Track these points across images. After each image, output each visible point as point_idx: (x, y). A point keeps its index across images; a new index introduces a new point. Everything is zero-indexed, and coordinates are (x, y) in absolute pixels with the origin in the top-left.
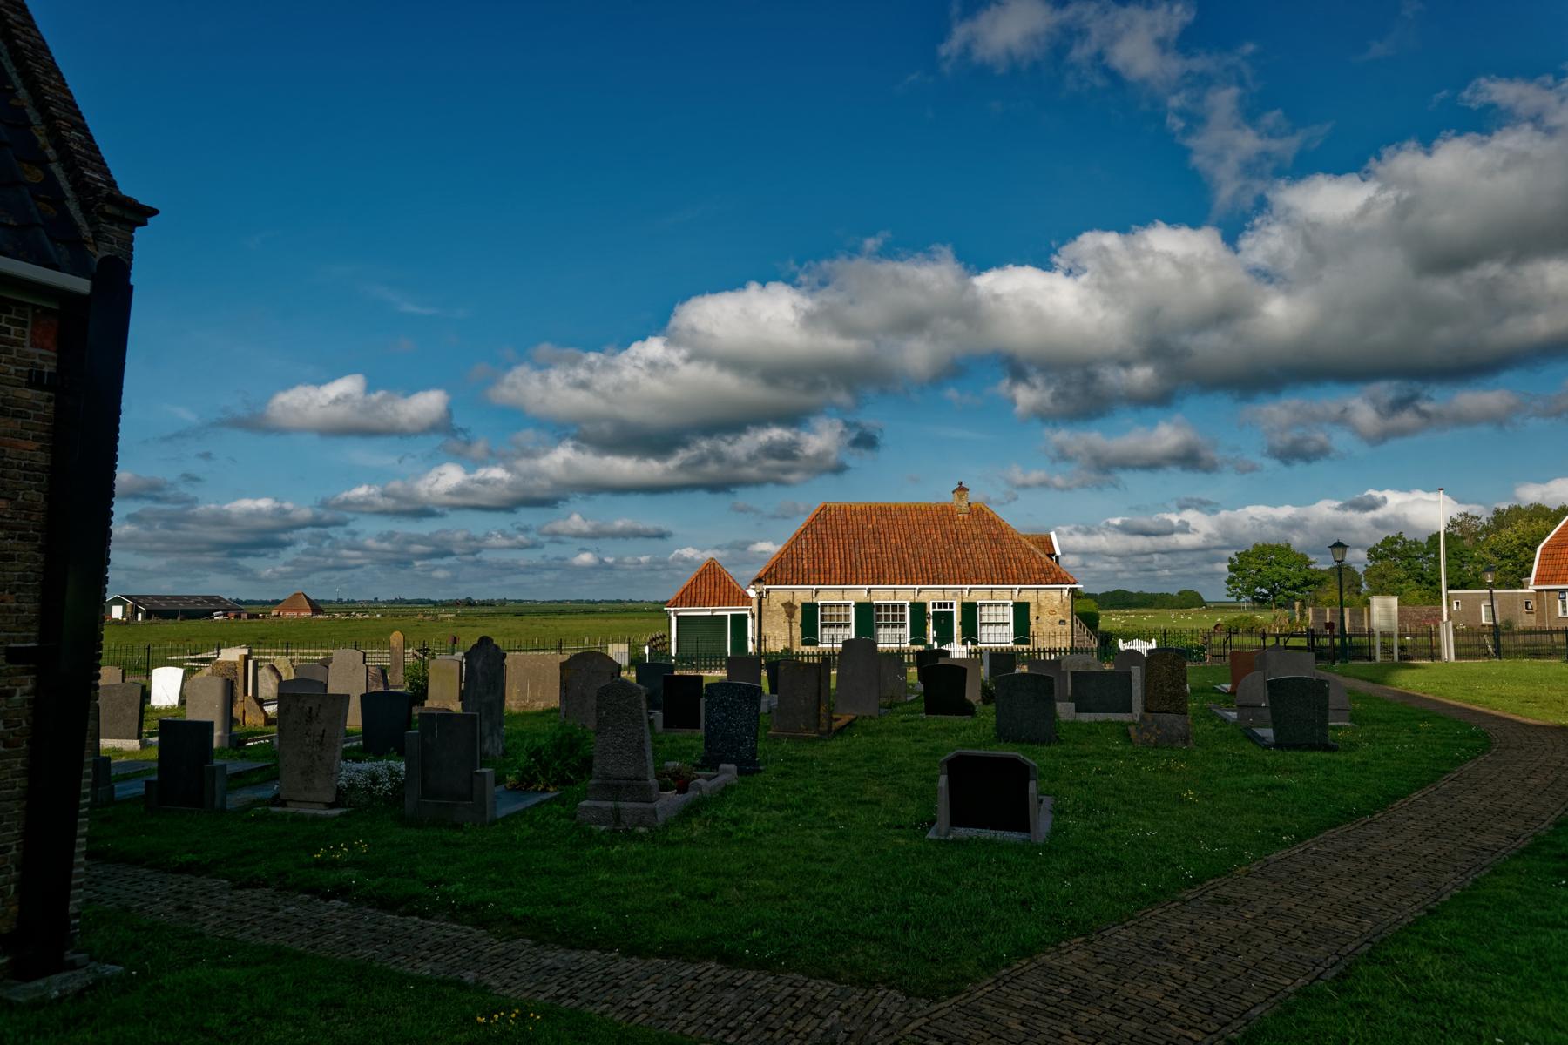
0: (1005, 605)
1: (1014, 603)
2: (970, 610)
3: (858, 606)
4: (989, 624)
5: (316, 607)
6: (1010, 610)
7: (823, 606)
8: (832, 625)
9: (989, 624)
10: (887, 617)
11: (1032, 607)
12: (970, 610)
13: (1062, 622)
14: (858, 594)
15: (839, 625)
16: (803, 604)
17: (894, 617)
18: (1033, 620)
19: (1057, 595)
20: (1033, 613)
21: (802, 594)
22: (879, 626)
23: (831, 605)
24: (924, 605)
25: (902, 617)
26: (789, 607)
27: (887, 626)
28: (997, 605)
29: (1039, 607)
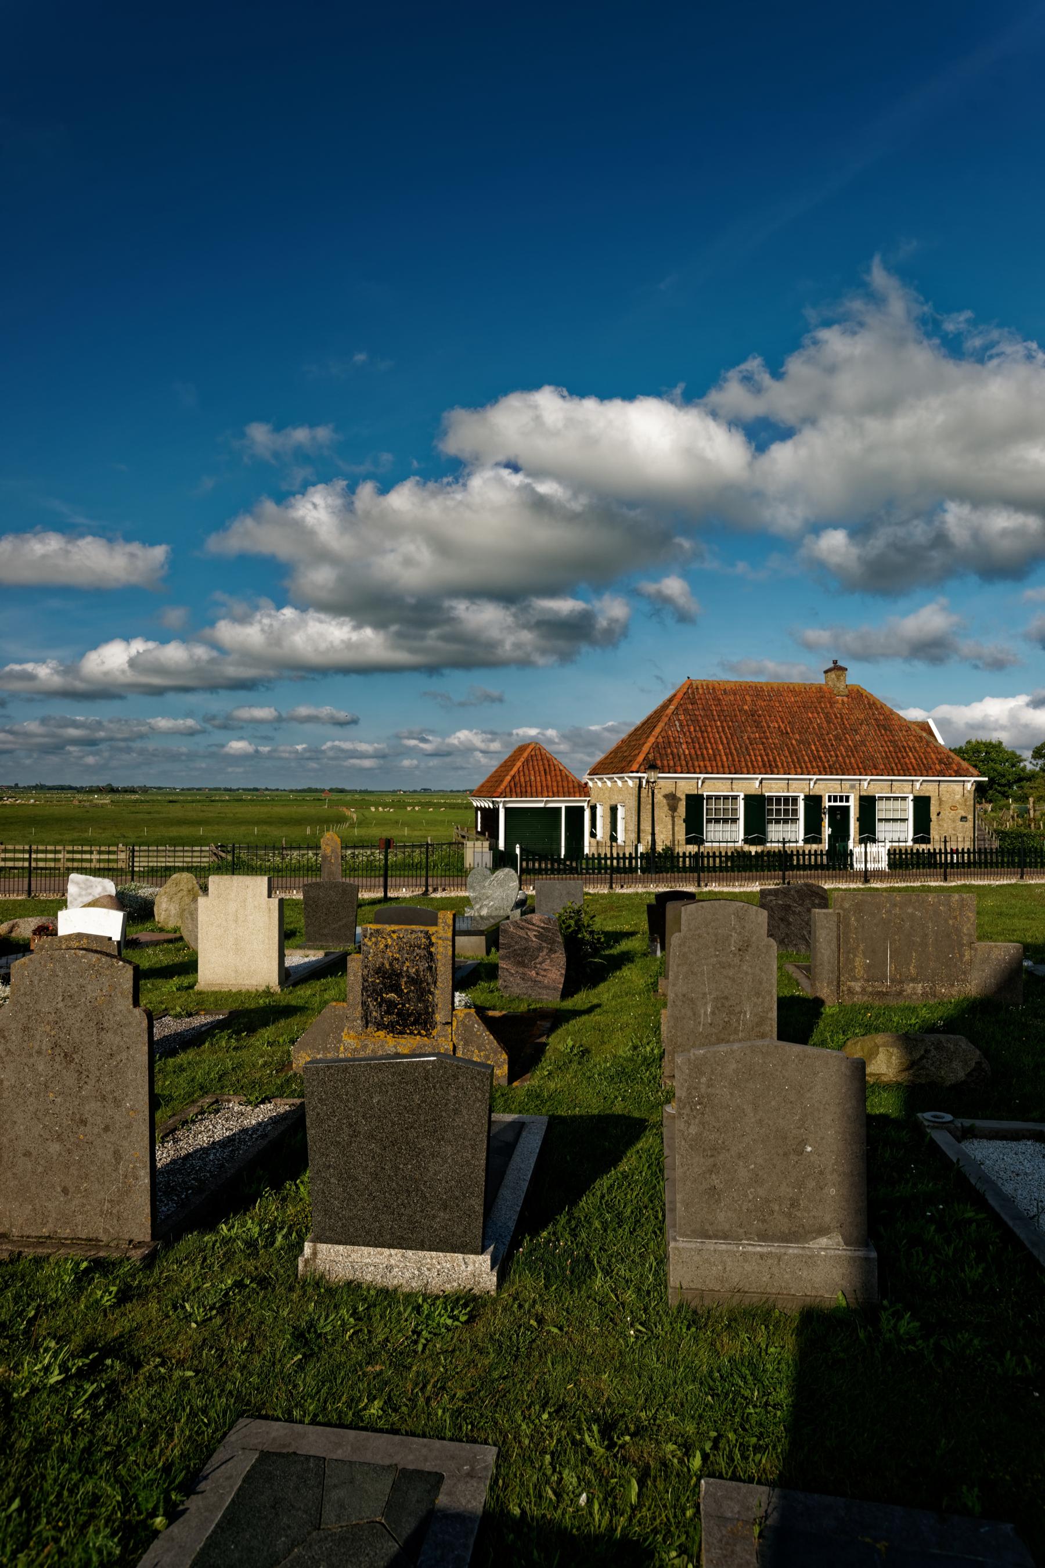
0: (904, 799)
1: (805, 796)
2: (868, 804)
3: (748, 798)
4: (887, 820)
6: (910, 805)
7: (709, 797)
8: (717, 821)
9: (887, 820)
10: (778, 811)
11: (933, 802)
12: (868, 804)
13: (964, 819)
14: (751, 784)
15: (725, 821)
16: (688, 797)
17: (786, 811)
18: (933, 816)
19: (958, 788)
20: (934, 809)
21: (686, 784)
22: (770, 821)
23: (718, 798)
24: (819, 799)
25: (795, 812)
26: (672, 799)
27: (778, 822)
28: (896, 799)
29: (940, 802)
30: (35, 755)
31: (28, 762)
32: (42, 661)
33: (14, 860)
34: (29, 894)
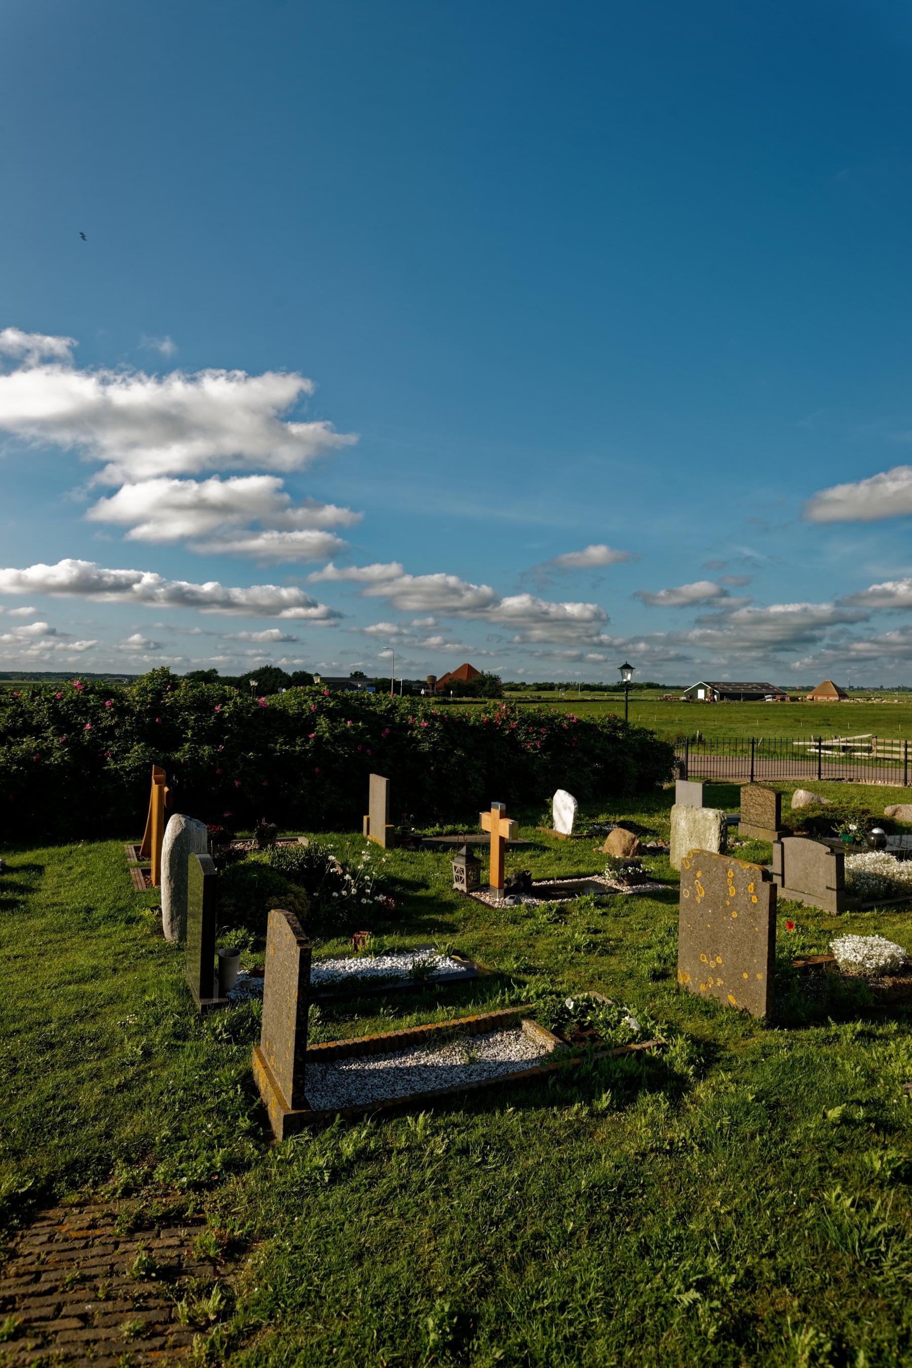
5: (842, 694)
30: (897, 661)
31: (891, 667)
32: (898, 579)
33: (892, 752)
34: (906, 783)
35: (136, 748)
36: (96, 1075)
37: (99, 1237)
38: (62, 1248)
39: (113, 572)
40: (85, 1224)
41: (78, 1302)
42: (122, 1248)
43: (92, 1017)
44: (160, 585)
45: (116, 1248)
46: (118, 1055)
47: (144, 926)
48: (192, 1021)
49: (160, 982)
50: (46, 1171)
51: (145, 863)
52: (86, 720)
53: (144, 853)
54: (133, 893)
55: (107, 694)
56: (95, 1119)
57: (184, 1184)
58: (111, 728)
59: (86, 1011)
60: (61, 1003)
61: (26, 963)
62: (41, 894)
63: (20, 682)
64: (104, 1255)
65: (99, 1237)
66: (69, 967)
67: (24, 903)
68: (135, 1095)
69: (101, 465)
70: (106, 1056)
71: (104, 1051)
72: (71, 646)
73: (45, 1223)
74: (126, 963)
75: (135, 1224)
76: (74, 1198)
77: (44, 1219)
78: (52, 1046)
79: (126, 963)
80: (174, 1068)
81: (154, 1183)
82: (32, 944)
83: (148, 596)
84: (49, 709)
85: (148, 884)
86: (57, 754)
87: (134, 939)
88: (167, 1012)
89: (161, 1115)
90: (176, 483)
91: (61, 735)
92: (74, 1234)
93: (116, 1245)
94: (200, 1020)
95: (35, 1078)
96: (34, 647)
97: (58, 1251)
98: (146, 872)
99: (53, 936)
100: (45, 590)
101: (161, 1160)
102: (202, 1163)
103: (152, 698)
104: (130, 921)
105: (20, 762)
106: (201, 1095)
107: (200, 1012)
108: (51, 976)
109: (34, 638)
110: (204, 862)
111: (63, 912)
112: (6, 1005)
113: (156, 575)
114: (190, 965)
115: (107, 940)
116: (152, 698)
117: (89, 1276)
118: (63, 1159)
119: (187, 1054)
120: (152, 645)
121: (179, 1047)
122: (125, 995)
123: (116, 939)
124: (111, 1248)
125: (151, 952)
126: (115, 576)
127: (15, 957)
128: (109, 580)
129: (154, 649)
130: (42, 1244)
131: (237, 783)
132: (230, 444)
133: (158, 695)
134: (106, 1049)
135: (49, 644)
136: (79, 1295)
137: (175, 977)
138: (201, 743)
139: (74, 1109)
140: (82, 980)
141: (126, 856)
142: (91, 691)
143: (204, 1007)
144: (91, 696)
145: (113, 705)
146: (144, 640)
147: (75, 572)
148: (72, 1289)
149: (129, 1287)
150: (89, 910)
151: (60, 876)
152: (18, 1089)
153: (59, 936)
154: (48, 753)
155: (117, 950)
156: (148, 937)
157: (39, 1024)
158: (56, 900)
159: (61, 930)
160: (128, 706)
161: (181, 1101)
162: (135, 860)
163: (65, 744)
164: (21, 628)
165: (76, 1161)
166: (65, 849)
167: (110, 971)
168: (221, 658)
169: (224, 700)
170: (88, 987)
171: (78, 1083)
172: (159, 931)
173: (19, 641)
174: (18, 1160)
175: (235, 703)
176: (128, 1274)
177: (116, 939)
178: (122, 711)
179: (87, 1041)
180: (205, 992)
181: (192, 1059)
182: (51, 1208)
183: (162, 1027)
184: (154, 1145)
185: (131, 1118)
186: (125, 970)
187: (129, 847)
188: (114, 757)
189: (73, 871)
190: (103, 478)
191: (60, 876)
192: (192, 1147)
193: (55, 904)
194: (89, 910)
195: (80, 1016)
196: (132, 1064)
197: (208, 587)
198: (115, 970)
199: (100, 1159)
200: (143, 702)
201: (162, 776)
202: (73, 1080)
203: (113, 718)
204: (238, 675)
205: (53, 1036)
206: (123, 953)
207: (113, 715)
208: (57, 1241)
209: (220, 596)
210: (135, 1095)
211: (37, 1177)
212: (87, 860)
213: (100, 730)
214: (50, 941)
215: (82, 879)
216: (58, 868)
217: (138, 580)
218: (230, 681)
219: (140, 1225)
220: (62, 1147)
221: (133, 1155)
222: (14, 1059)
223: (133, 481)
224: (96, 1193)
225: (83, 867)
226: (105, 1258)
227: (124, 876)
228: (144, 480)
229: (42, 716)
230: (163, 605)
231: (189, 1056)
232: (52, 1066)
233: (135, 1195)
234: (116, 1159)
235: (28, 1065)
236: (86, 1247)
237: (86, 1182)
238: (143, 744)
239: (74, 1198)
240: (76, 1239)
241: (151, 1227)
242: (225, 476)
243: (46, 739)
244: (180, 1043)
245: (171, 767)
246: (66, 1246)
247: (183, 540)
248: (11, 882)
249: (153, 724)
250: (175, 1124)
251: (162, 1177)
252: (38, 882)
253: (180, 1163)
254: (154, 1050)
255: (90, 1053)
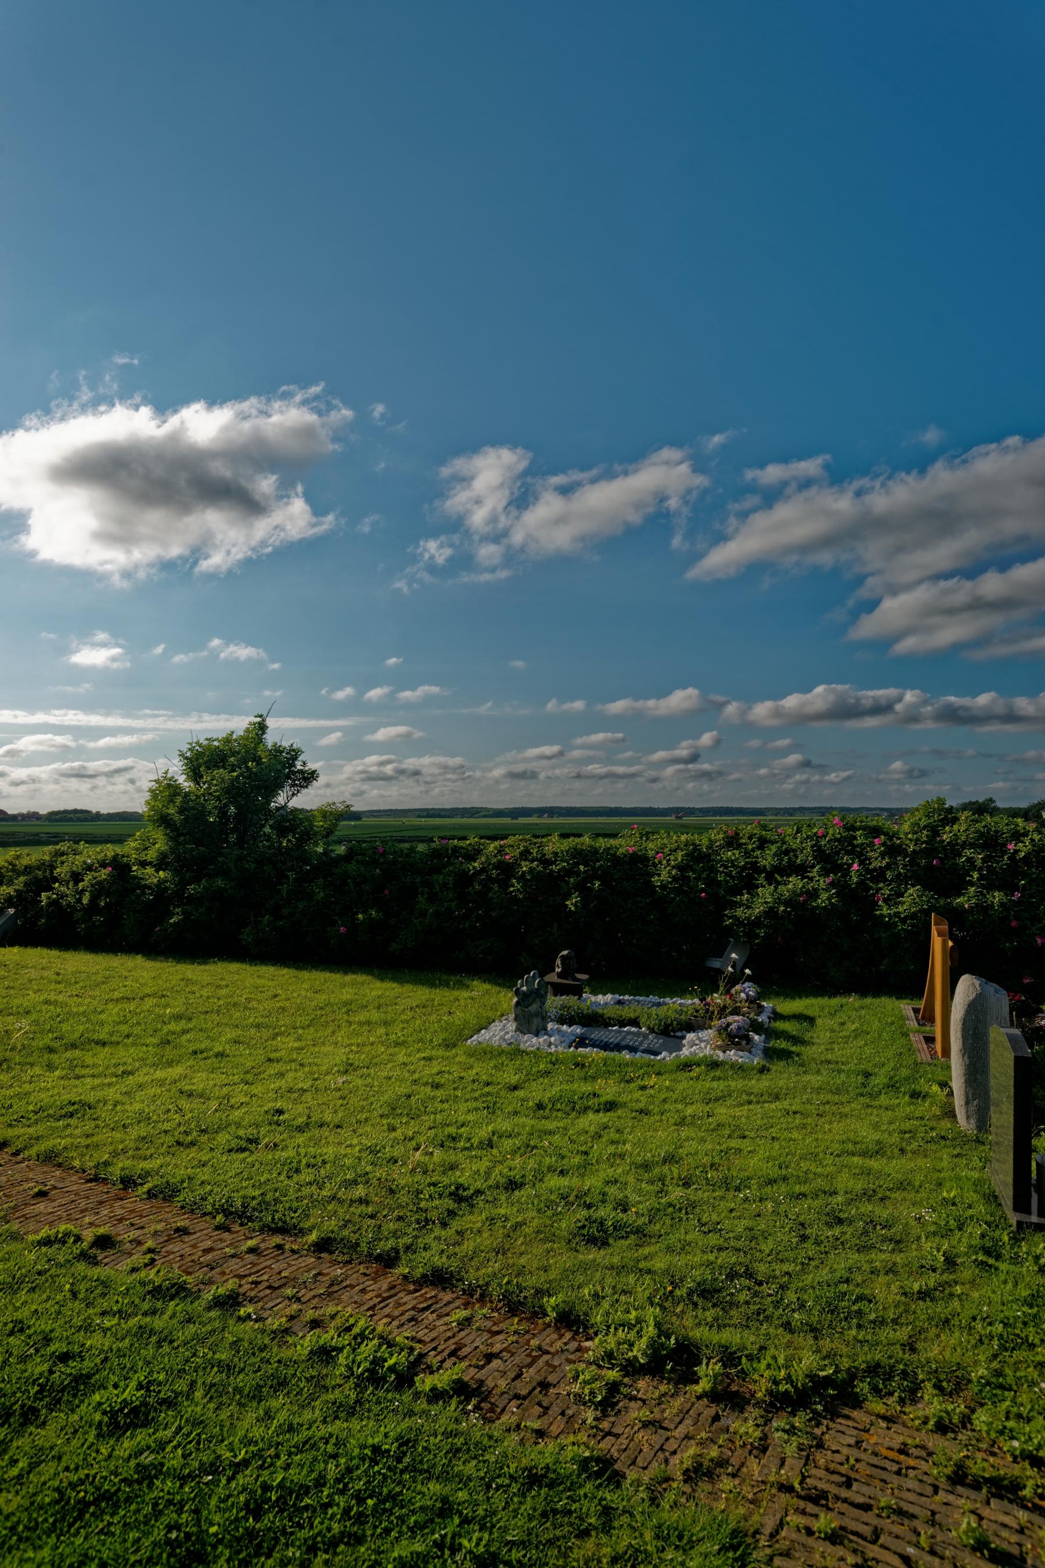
35: (911, 891)
36: (891, 1270)
37: (914, 1468)
38: (871, 1462)
39: (871, 693)
40: (897, 1447)
41: (897, 1537)
42: (942, 1496)
43: (882, 1199)
44: (925, 702)
45: (936, 1492)
46: (914, 1253)
47: (931, 1104)
48: (1006, 1238)
49: (958, 1178)
50: (845, 1363)
51: (928, 1028)
52: (853, 860)
53: (926, 1017)
54: (916, 1064)
55: (875, 831)
56: (895, 1321)
57: (1015, 1449)
58: (882, 871)
59: (874, 1191)
60: (845, 1175)
61: (805, 1121)
62: (814, 1048)
63: (774, 818)
64: (921, 1495)
65: (914, 1468)
66: (852, 1135)
67: (798, 1055)
68: (940, 1309)
69: (860, 580)
70: (901, 1251)
71: (898, 1243)
72: (827, 778)
73: (850, 1423)
74: (914, 1145)
75: (955, 1473)
76: (879, 1408)
77: (848, 1417)
78: (840, 1221)
79: (914, 1145)
80: (986, 1291)
81: (973, 1430)
82: (809, 1101)
83: (912, 717)
84: (812, 846)
85: (933, 1056)
86: (824, 896)
87: (922, 1118)
88: (971, 1217)
89: (975, 1347)
90: (943, 584)
91: (827, 875)
92: (885, 1452)
93: (936, 1489)
94: (1016, 1240)
95: (826, 1253)
96: (789, 781)
97: (868, 1464)
98: (930, 1040)
99: (829, 1097)
100: (802, 719)
101: (982, 1405)
102: (1039, 1432)
103: (927, 836)
104: (915, 1095)
105: (787, 903)
106: (1027, 1336)
107: (1014, 1228)
108: (832, 1141)
109: (789, 772)
110: (1011, 1038)
111: (839, 1071)
112: (790, 1162)
113: (918, 692)
114: (996, 1165)
115: (890, 1113)
116: (927, 836)
117: (907, 1512)
118: (865, 1357)
119: (1002, 1277)
120: (916, 773)
121: (991, 1266)
122: (917, 1184)
123: (900, 1113)
124: (929, 1490)
125: (943, 1138)
126: (872, 697)
127: (795, 1113)
128: (867, 703)
129: (919, 777)
130: (849, 1446)
131: (1039, 941)
132: (1011, 527)
133: (935, 831)
134: (898, 1242)
135: (804, 777)
136: (897, 1529)
137: (976, 1175)
138: (991, 888)
139: (870, 1301)
140: (864, 1154)
141: (903, 1018)
142: (854, 829)
143: (1020, 1224)
144: (858, 833)
145: (884, 844)
146: (907, 767)
147: (831, 698)
148: (889, 1517)
149: (958, 1552)
150: (867, 1075)
151: (833, 1031)
152: (810, 1259)
153: (836, 1098)
154: (814, 894)
155: (903, 1127)
156: (938, 1118)
157: (825, 1192)
158: (830, 1057)
159: (837, 1092)
160: (900, 846)
161: (1001, 1336)
162: (913, 1024)
163: (832, 884)
164: (778, 762)
165: (878, 1365)
166: (836, 1001)
167: (896, 1151)
168: (1000, 784)
169: (1018, 836)
170: (874, 1164)
171: (872, 1272)
172: (951, 1114)
173: (775, 775)
174: (816, 1338)
175: (1032, 840)
176: (954, 1533)
177: (900, 1113)
178: (893, 850)
179: (878, 1227)
180: (1021, 1204)
181: (1010, 1286)
182: (854, 1408)
183: (966, 1235)
184: (970, 1381)
185: (938, 1336)
186: (914, 1152)
187: (906, 1007)
188: (885, 901)
189: (845, 1027)
190: (864, 593)
191: (833, 1031)
192: (1022, 1405)
193: (829, 1062)
194: (867, 1075)
195: (868, 1195)
196: (934, 1271)
197: (983, 699)
198: (902, 1150)
199: (904, 1374)
200: (917, 840)
201: (945, 927)
202: (866, 1267)
203: (883, 858)
204: (1024, 805)
205: (841, 1211)
206: (910, 1132)
207: (883, 855)
208: (865, 1450)
209: (1000, 709)
210: (940, 1309)
211: (837, 1366)
212: (860, 1017)
213: (868, 871)
214: (828, 1103)
215: (856, 1037)
216: (830, 1022)
217: (900, 699)
218: (1014, 813)
219: (959, 1477)
220: (861, 1342)
221: (944, 1384)
222: (802, 1225)
223: (894, 590)
224: (904, 1413)
225: (856, 1025)
226: (924, 1499)
227: (903, 1041)
228: (910, 587)
229: (806, 855)
230: (930, 725)
231: (1005, 1282)
232: (842, 1243)
233: (952, 1435)
234: (923, 1381)
235: (817, 1235)
236: (898, 1473)
237: (891, 1394)
238: (918, 887)
239: (879, 1408)
240: (886, 1458)
241: (976, 1486)
242: (1004, 566)
243: (811, 879)
244: (991, 1261)
245: (955, 918)
246: (875, 1461)
247: (957, 647)
248: (783, 1031)
249: (929, 867)
250: (995, 1365)
251: (985, 1428)
252: (810, 1034)
253: (1007, 1418)
254: (959, 1261)
255: (883, 1241)
